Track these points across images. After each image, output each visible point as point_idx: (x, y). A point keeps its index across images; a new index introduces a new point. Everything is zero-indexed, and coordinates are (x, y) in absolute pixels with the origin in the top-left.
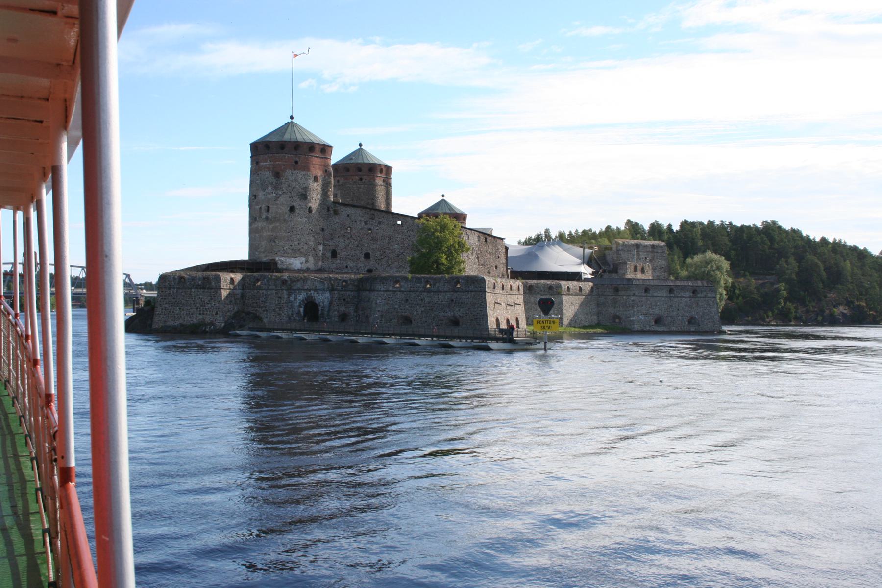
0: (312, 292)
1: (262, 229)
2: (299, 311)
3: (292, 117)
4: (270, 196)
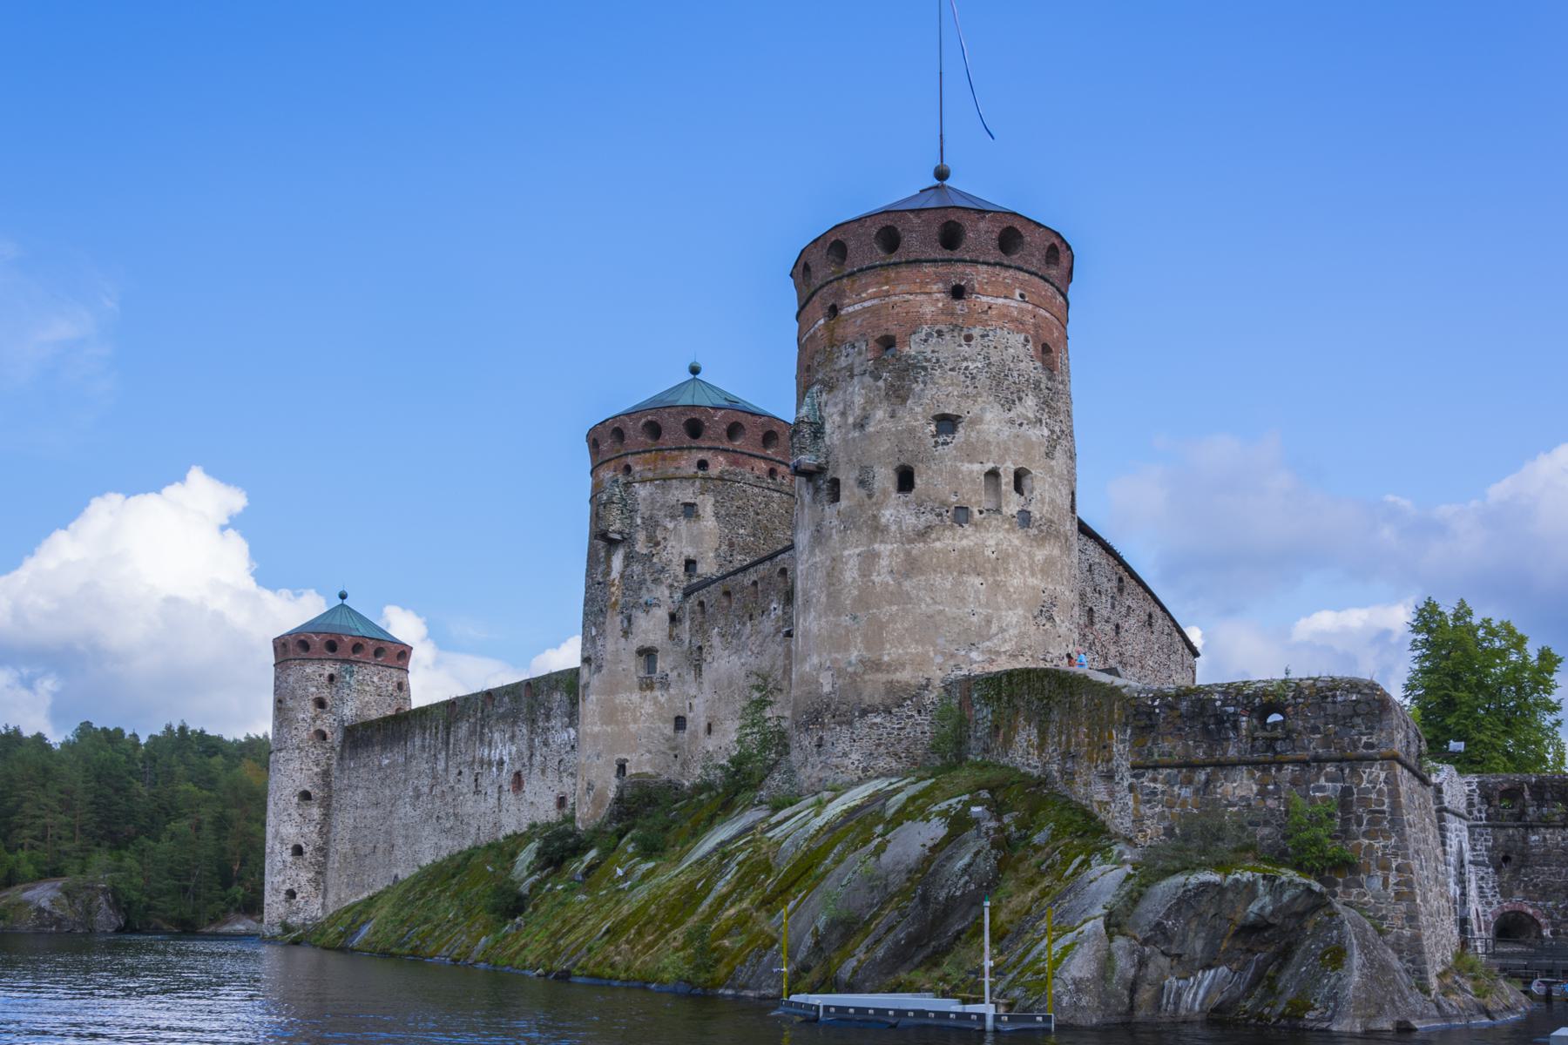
1: (1003, 558)
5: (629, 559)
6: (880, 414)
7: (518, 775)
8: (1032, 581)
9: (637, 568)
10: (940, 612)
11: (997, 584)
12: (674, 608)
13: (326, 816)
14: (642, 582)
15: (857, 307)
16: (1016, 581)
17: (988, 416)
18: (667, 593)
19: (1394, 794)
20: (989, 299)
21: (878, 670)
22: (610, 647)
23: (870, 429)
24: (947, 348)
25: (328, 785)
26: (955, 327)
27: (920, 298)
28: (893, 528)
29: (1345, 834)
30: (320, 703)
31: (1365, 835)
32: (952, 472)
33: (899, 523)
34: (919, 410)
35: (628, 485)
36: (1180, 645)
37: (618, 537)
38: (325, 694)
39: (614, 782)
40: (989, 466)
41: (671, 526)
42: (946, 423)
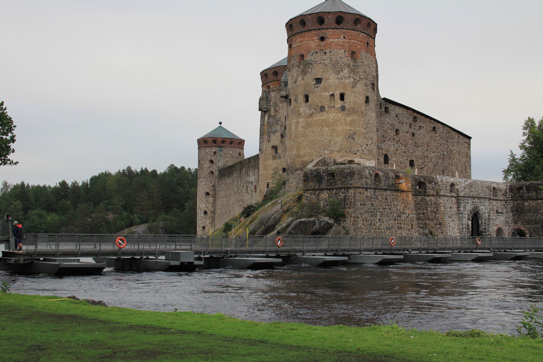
0: (476, 200)
2: (468, 225)
4: (347, 81)
5: (269, 117)
6: (300, 79)
7: (255, 186)
8: (345, 128)
9: (271, 120)
10: (316, 139)
11: (333, 130)
12: (282, 132)
13: (215, 200)
14: (273, 124)
16: (340, 128)
17: (331, 77)
18: (280, 127)
19: (355, 197)
21: (299, 157)
22: (265, 146)
23: (297, 84)
24: (318, 57)
25: (215, 190)
26: (321, 50)
27: (311, 42)
28: (303, 114)
29: (344, 208)
30: (212, 162)
31: (348, 208)
32: (320, 96)
33: (304, 112)
34: (310, 77)
35: (269, 92)
36: (456, 136)
37: (266, 110)
38: (213, 158)
39: (266, 189)
40: (331, 93)
41: (281, 105)
42: (319, 81)
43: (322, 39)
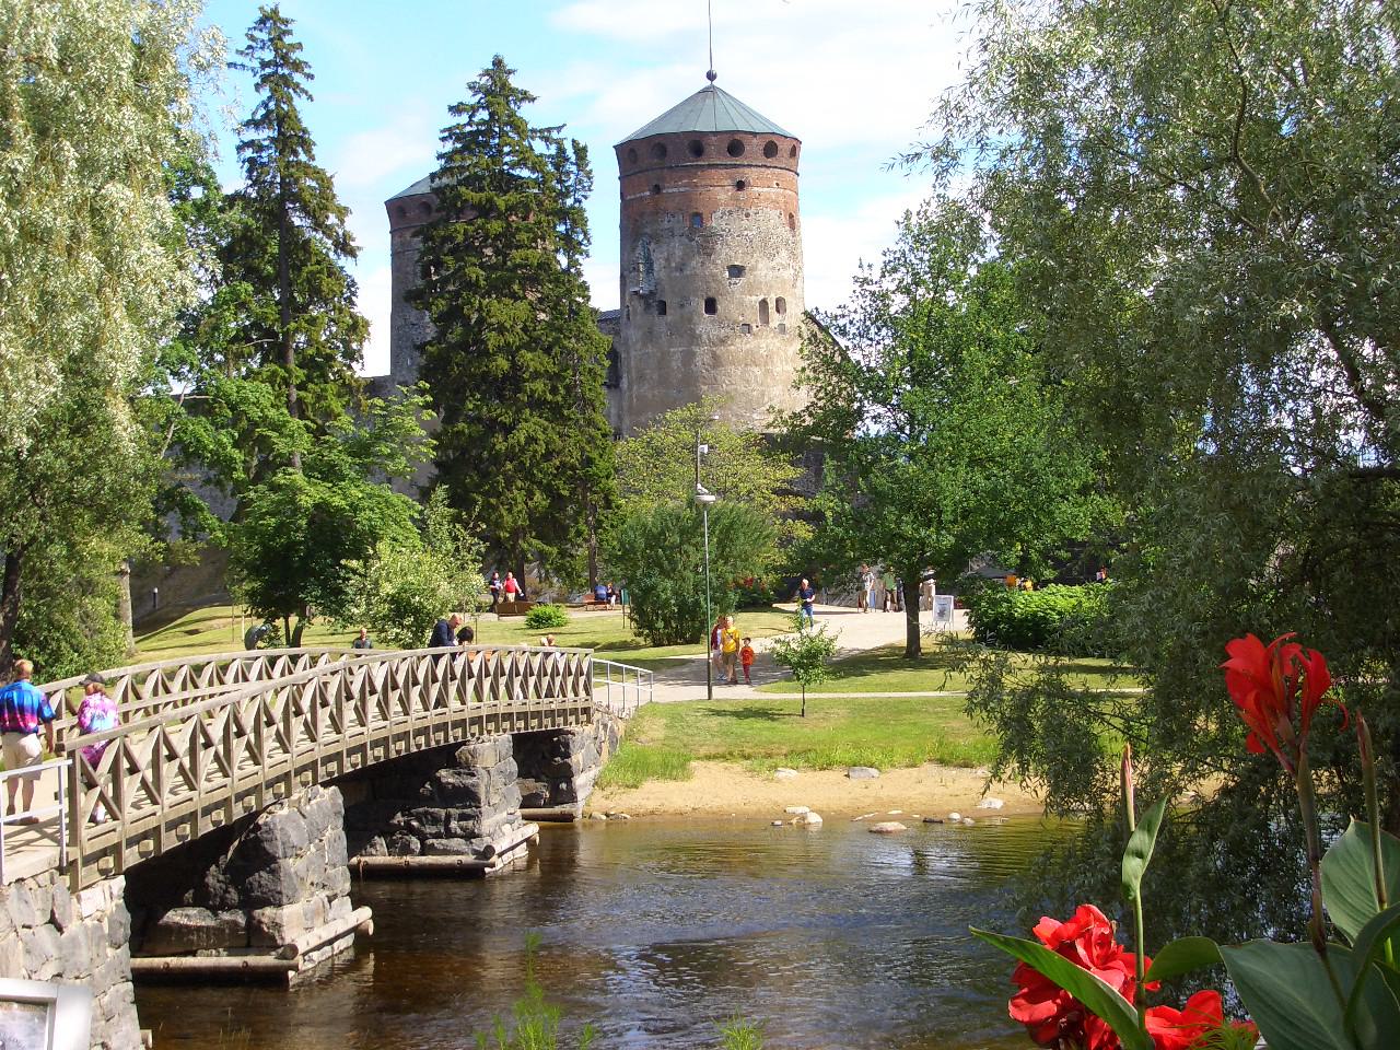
3: (711, 76)
15: (675, 190)
17: (760, 266)
20: (760, 190)
23: (687, 272)
24: (739, 224)
28: (705, 336)
32: (740, 301)
40: (761, 298)
42: (736, 271)
43: (740, 186)
